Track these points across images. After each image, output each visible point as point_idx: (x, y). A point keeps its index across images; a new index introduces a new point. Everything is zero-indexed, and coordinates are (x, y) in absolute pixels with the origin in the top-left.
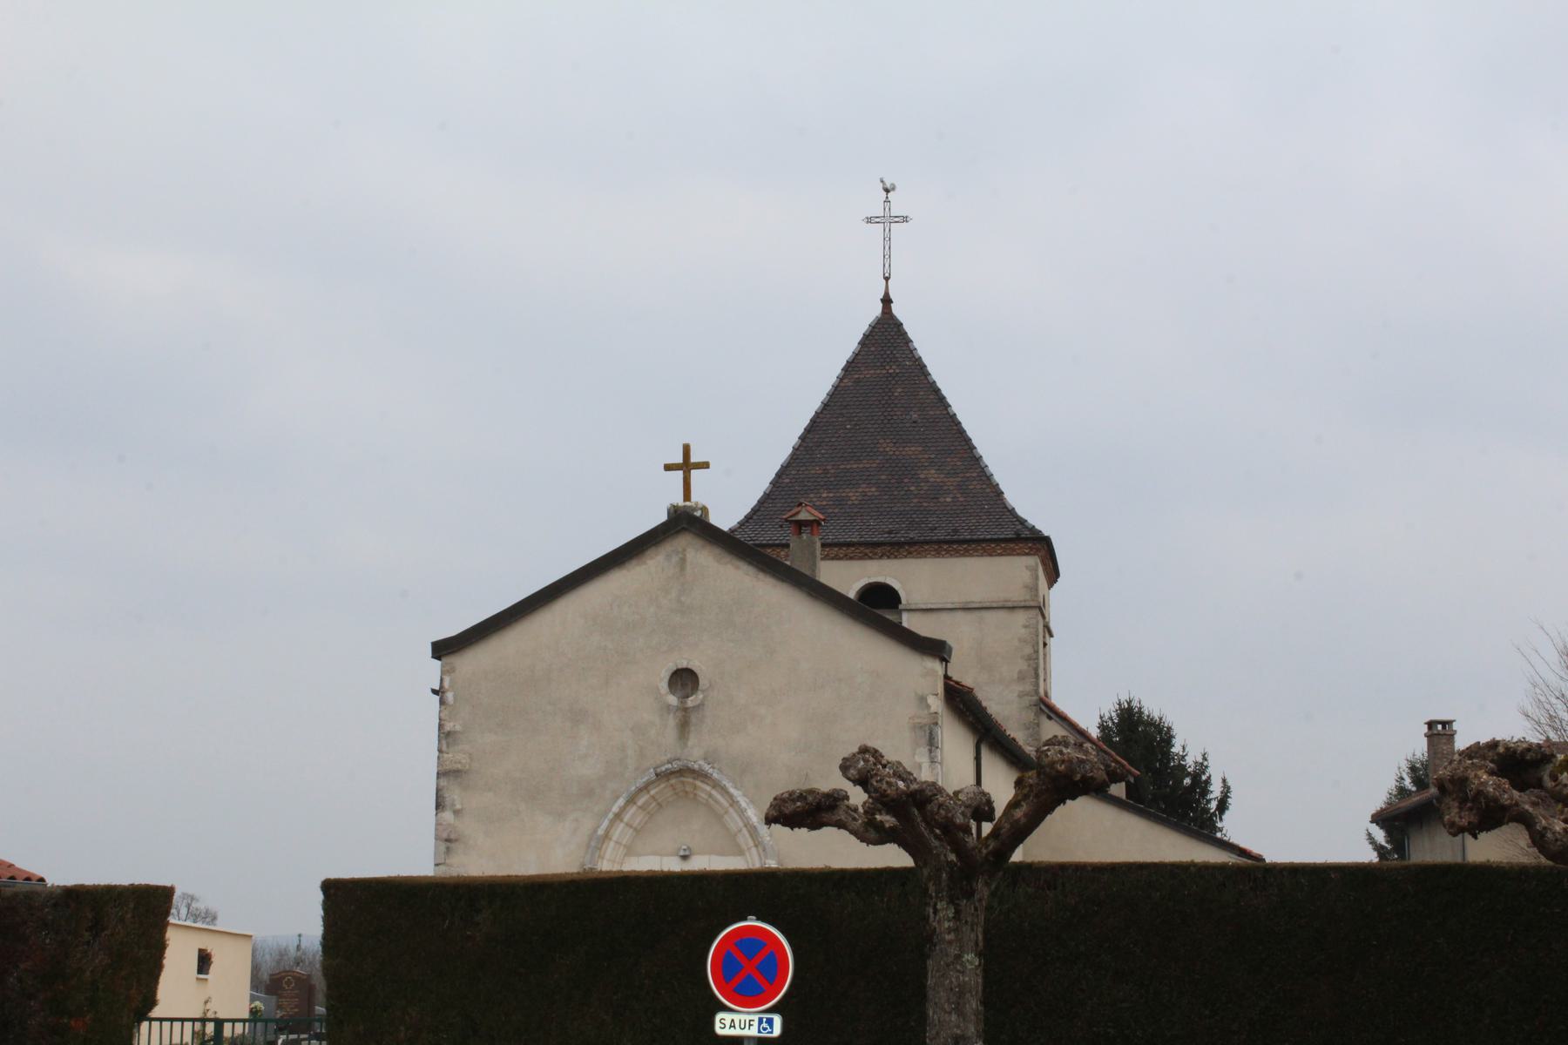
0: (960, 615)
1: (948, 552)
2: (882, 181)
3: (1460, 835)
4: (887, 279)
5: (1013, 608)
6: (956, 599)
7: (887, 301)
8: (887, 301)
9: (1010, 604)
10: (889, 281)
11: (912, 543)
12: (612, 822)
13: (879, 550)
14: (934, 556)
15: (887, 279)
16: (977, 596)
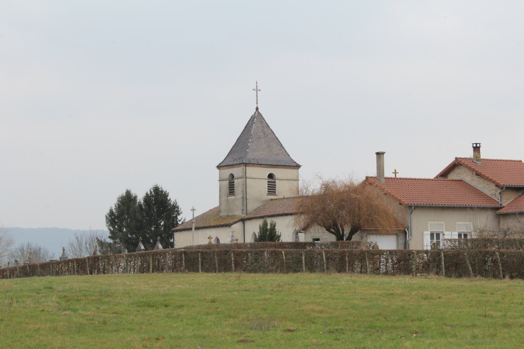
0: (286, 181)
1: (278, 167)
2: (257, 81)
3: (195, 217)
4: (257, 103)
5: (295, 180)
6: (285, 178)
7: (257, 109)
8: (257, 109)
9: (294, 179)
10: (258, 104)
11: (279, 165)
12: (375, 230)
13: (273, 167)
14: (282, 168)
15: (257, 103)
16: (289, 177)
